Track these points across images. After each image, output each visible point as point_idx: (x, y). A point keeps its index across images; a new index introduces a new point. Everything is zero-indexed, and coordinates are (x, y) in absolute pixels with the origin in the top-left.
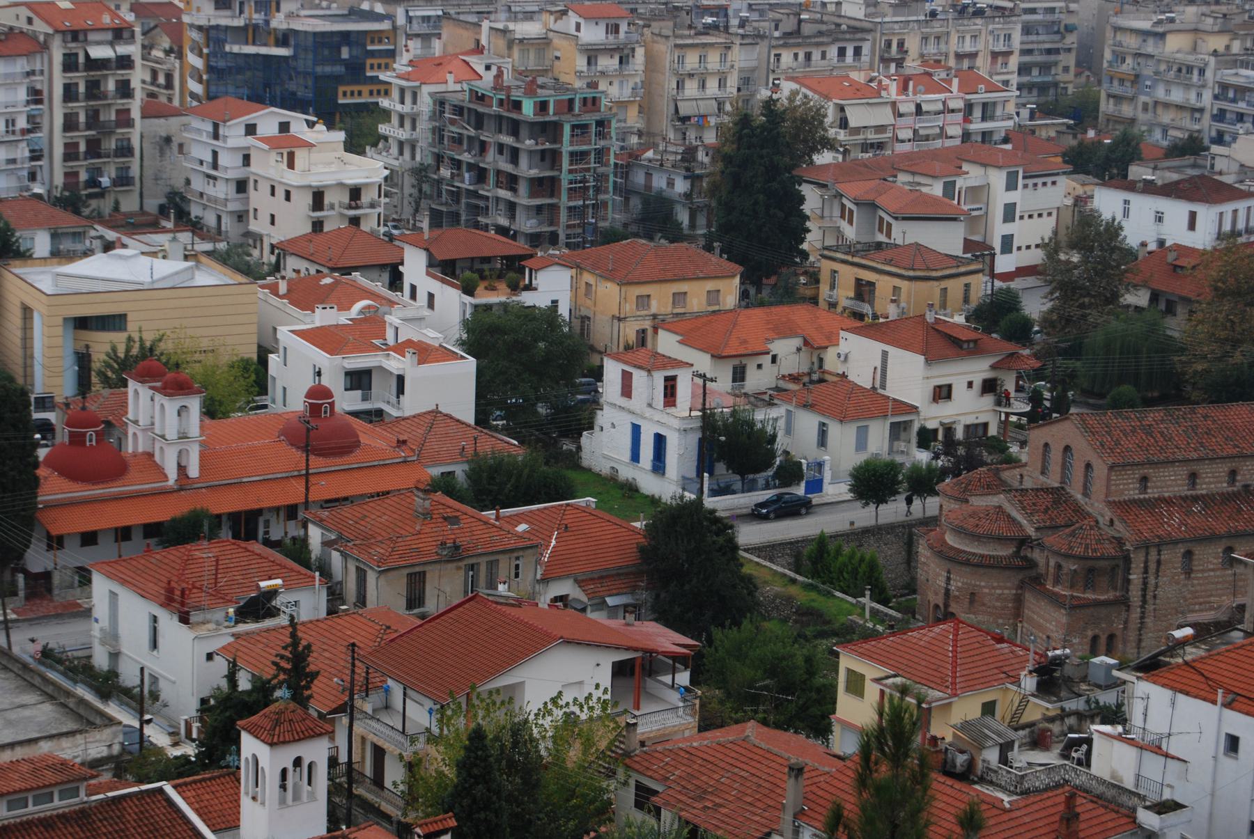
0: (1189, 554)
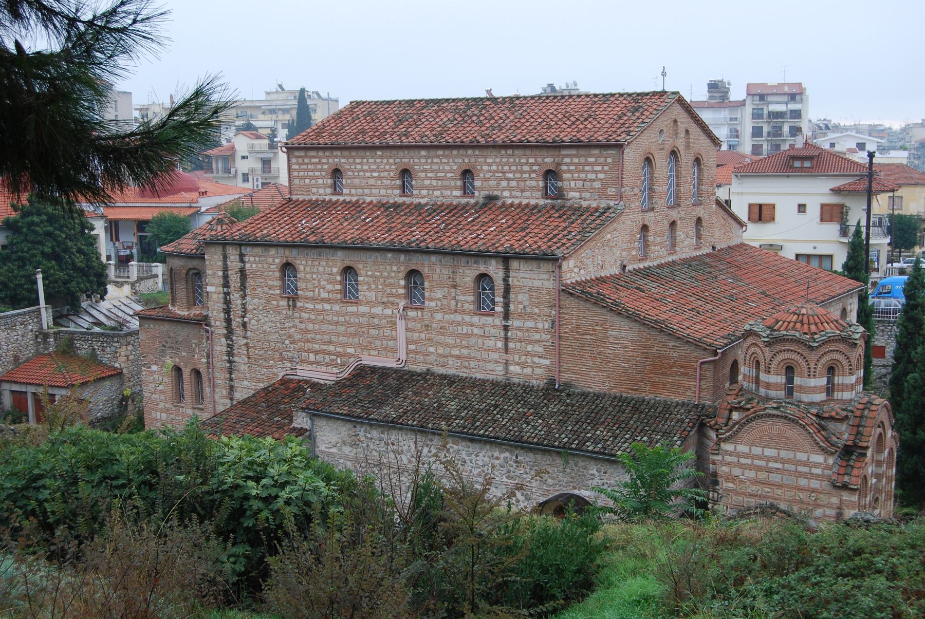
0: (287, 268)
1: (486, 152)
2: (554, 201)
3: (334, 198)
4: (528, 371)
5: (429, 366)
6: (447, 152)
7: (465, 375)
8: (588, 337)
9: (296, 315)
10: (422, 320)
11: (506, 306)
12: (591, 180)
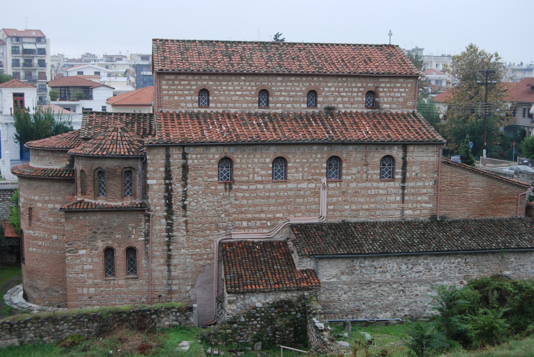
0: (226, 162)
1: (327, 79)
2: (374, 110)
3: (202, 110)
4: (418, 212)
5: (343, 218)
6: (298, 79)
7: (372, 221)
8: (457, 188)
9: (232, 195)
10: (340, 188)
11: (404, 174)
12: (397, 97)
